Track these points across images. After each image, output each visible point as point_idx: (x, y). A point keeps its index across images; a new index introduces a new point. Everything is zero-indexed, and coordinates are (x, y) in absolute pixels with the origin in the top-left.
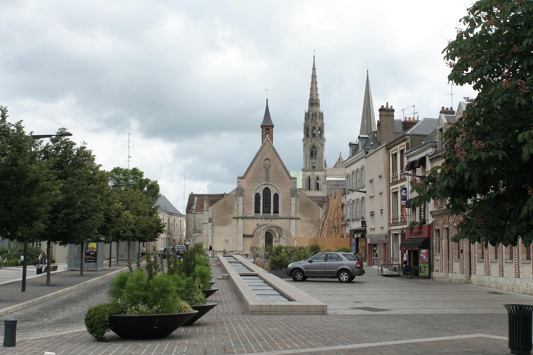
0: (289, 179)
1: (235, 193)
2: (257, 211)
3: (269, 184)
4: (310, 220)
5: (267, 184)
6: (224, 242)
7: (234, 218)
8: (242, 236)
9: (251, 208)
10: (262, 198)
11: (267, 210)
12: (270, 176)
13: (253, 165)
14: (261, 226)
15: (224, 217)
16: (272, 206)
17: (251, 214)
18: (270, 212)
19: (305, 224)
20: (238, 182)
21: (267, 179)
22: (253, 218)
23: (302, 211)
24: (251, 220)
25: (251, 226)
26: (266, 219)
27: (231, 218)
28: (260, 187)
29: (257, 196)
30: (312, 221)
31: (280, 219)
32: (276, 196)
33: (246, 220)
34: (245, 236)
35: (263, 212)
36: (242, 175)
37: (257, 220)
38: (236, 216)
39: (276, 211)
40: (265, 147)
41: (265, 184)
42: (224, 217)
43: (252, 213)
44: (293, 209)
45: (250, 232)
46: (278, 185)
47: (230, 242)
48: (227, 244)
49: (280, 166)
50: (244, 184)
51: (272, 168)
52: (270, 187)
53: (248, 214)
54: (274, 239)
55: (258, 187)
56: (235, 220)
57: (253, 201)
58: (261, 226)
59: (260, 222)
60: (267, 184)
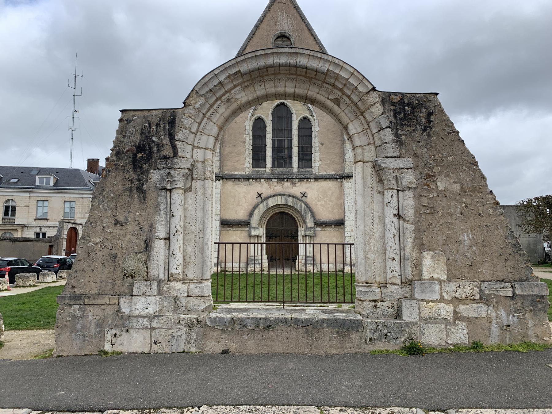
8: (218, 223)
10: (269, 129)
16: (295, 150)
17: (244, 169)
18: (290, 164)
22: (247, 178)
25: (244, 199)
26: (280, 179)
29: (259, 125)
31: (317, 179)
32: (305, 124)
33: (230, 184)
34: (225, 224)
35: (273, 166)
43: (245, 165)
45: (240, 215)
52: (288, 103)
53: (235, 171)
54: (301, 232)
57: (248, 137)
59: (264, 188)
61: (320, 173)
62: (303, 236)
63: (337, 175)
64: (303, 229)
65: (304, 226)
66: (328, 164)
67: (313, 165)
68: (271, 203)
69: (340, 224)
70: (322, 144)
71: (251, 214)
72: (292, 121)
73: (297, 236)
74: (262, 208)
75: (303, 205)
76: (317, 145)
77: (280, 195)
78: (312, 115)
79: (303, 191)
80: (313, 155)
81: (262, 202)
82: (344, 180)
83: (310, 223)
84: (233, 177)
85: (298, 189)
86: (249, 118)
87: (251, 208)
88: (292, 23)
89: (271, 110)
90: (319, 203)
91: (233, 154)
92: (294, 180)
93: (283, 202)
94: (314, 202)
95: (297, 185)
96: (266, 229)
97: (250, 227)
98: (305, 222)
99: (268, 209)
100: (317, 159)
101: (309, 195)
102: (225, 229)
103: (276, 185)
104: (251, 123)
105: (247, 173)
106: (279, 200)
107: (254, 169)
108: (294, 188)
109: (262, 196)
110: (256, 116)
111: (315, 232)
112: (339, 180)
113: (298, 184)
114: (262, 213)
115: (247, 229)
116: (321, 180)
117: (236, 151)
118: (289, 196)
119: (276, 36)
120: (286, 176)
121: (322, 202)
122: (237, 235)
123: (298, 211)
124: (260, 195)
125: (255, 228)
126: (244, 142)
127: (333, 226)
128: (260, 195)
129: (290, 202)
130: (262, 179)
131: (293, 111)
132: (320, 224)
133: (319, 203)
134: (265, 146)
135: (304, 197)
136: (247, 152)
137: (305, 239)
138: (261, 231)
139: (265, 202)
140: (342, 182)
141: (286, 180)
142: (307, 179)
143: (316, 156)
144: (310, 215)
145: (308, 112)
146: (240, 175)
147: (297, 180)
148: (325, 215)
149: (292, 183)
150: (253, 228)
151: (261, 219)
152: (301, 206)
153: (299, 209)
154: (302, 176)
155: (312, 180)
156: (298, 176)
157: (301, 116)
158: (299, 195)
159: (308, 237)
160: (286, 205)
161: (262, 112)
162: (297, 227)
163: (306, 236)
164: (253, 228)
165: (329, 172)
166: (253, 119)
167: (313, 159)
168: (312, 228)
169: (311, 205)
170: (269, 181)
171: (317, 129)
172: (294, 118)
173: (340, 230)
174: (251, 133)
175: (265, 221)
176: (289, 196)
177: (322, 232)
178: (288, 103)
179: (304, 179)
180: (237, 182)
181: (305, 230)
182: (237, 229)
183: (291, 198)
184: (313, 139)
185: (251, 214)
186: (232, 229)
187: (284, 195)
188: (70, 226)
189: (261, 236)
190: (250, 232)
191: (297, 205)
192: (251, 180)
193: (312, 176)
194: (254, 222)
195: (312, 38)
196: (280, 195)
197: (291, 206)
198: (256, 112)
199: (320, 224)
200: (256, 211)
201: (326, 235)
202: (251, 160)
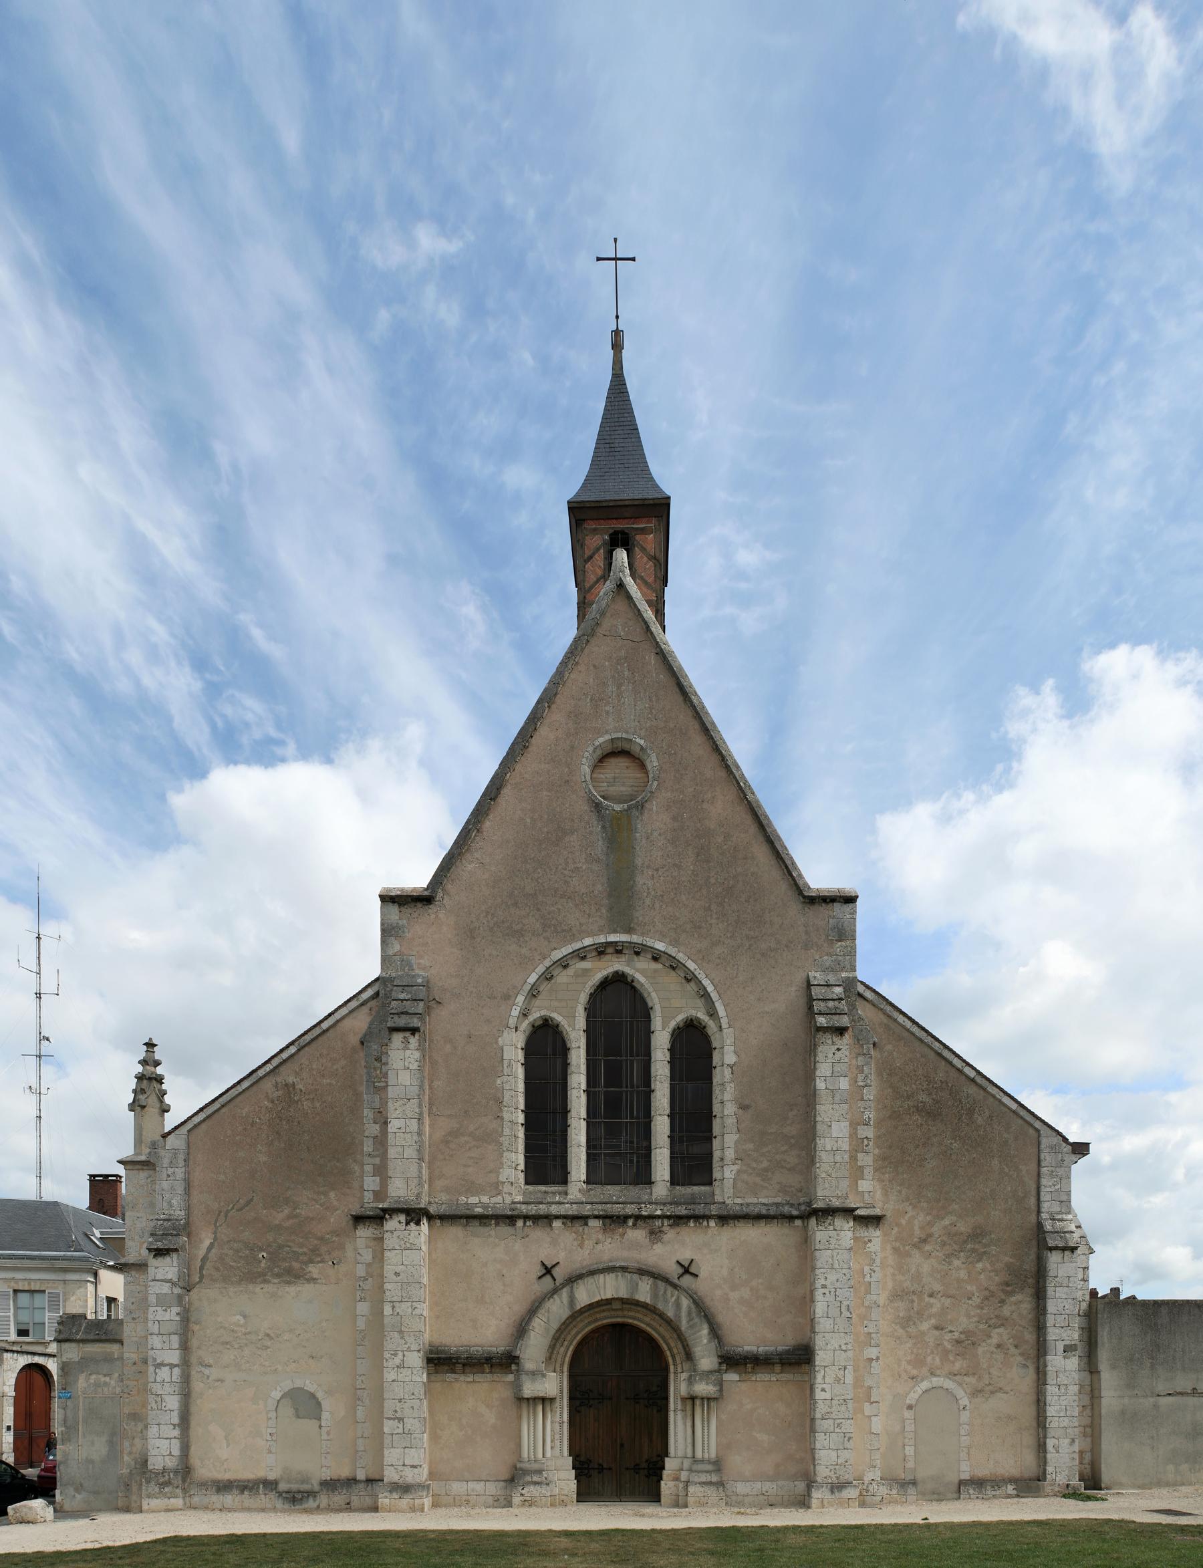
0: (794, 908)
1: (361, 1022)
2: (545, 1163)
3: (638, 951)
4: (963, 1227)
5: (618, 949)
6: (287, 1410)
7: (359, 1219)
8: (416, 1360)
9: (490, 1138)
10: (578, 1058)
11: (620, 1157)
12: (642, 881)
13: (506, 791)
14: (574, 1279)
15: (279, 1217)
16: (661, 1126)
17: (496, 1188)
19: (924, 1265)
20: (388, 932)
21: (621, 902)
23: (897, 1158)
24: (495, 1232)
26: (614, 1221)
27: (338, 1218)
28: (563, 977)
29: (545, 1044)
30: (977, 1234)
31: (725, 1219)
34: (441, 1362)
36: (418, 878)
37: (538, 1234)
38: (370, 1204)
39: (694, 1164)
40: (599, 648)
41: (601, 951)
42: (279, 1217)
44: (835, 1132)
45: (486, 1331)
46: (702, 957)
47: (333, 1409)
48: (309, 1425)
49: (721, 806)
50: (435, 952)
51: (655, 822)
52: (639, 971)
53: (472, 1189)
54: (678, 1386)
55: (547, 977)
56: (364, 1233)
58: (574, 1279)
59: (565, 1248)
60: (618, 949)
61: (739, 1201)
62: (684, 1399)
63: (792, 1205)
64: (684, 1375)
65: (686, 1366)
66: (766, 1170)
67: (716, 1174)
68: (584, 1295)
69: (799, 1359)
70: (744, 1107)
71: (521, 1330)
72: (648, 1033)
73: (666, 1399)
74: (558, 1309)
75: (685, 1302)
76: (730, 1109)
77: (612, 1269)
78: (713, 1013)
79: (685, 1255)
80: (716, 1143)
81: (555, 1291)
82: (813, 1221)
83: (707, 1361)
84: (464, 1211)
85: (670, 1250)
86: (512, 1022)
87: (520, 1308)
88: (651, 708)
89: (583, 998)
90: (734, 1296)
91: (463, 1139)
92: (658, 1223)
93: (623, 1293)
94: (718, 1292)
95: (666, 1237)
96: (571, 1376)
97: (519, 1372)
98: (689, 1356)
99: (576, 1315)
100: (730, 1154)
101: (704, 1268)
102: (439, 1377)
103: (600, 1236)
104: (520, 1039)
105: (508, 1200)
106: (610, 1287)
107: (530, 1188)
108: (658, 1248)
109: (555, 1272)
110: (535, 1015)
111: (720, 1384)
112: (798, 1222)
113: (670, 1234)
114: (555, 1325)
115: (511, 1377)
116: (741, 1224)
117: (472, 1128)
118: (642, 1272)
119: (599, 752)
120: (630, 1210)
121: (745, 1293)
122: (479, 1397)
123: (668, 1321)
124: (548, 1271)
125: (533, 1373)
126: (500, 1103)
127: (778, 1368)
128: (548, 1271)
129: (644, 1291)
130: (557, 1217)
131: (654, 999)
132: (732, 1361)
133: (734, 1296)
134: (565, 1112)
135: (687, 1278)
136: (507, 1131)
137: (689, 1408)
138: (553, 1384)
139: (565, 1293)
140: (806, 1228)
141: (630, 1222)
142: (698, 1218)
143: (728, 1143)
144: (705, 1331)
145: (700, 1003)
146: (485, 1206)
147: (666, 1222)
148: (750, 1335)
149: (652, 1233)
150: (527, 1373)
151: (552, 1347)
152: (678, 1305)
153: (670, 1314)
154: (682, 1210)
155: (712, 1223)
156: (669, 1210)
157: (680, 1018)
158: (673, 1270)
159: (698, 1402)
160: (629, 1303)
161: (556, 1004)
162: (667, 1369)
163: (693, 1399)
164: (527, 1373)
165: (765, 1199)
166: (525, 1025)
167: (717, 1154)
168: (711, 1372)
169: (708, 1301)
170: (578, 1227)
171: (730, 1058)
172: (657, 1022)
173: (798, 1377)
174: (520, 1072)
175: (566, 1352)
176: (642, 1272)
177: (744, 1386)
178: (638, 976)
179: (688, 1217)
180: (475, 1226)
181: (690, 1381)
182: (478, 1377)
183: (645, 1278)
184: (716, 1091)
185: (521, 1330)
186: (462, 1378)
187: (624, 1269)
188: (24, 1360)
189: (552, 1400)
190: (517, 1386)
191: (666, 1301)
192: (520, 1223)
193: (714, 1210)
194: (533, 1350)
195: (715, 758)
196: (612, 1269)
197: (644, 1306)
198: (537, 1003)
199: (732, 1361)
200: (537, 1323)
201: (750, 1396)
202: (521, 1160)
